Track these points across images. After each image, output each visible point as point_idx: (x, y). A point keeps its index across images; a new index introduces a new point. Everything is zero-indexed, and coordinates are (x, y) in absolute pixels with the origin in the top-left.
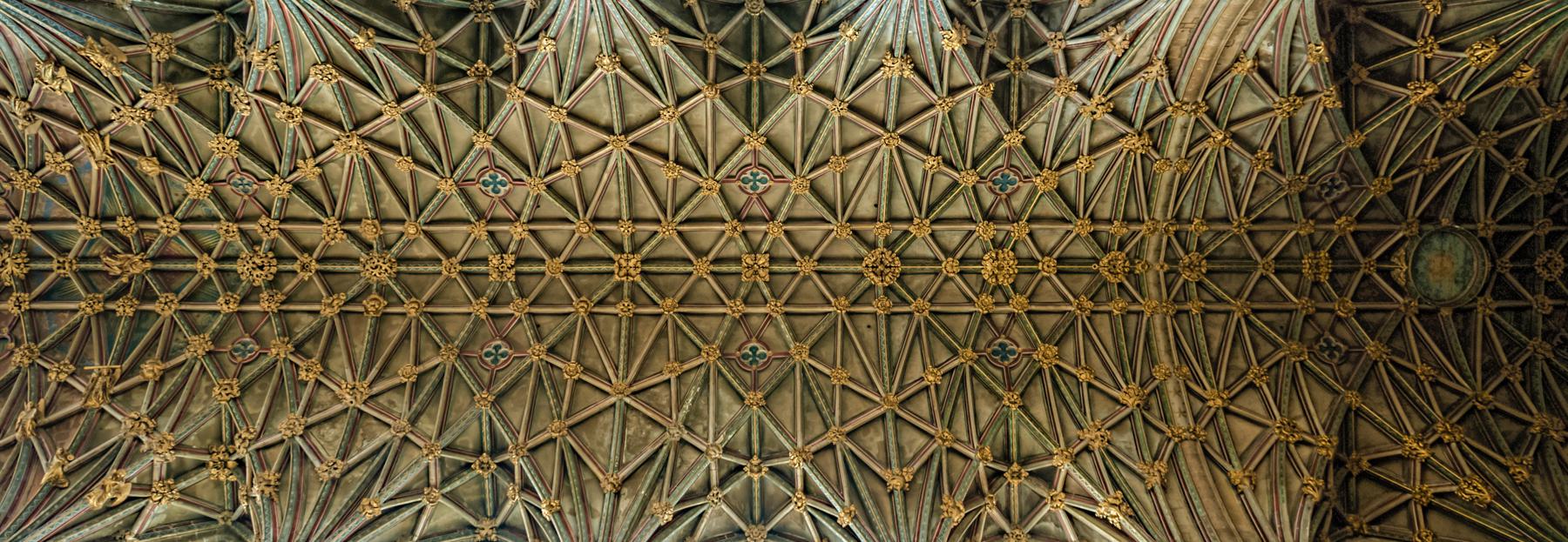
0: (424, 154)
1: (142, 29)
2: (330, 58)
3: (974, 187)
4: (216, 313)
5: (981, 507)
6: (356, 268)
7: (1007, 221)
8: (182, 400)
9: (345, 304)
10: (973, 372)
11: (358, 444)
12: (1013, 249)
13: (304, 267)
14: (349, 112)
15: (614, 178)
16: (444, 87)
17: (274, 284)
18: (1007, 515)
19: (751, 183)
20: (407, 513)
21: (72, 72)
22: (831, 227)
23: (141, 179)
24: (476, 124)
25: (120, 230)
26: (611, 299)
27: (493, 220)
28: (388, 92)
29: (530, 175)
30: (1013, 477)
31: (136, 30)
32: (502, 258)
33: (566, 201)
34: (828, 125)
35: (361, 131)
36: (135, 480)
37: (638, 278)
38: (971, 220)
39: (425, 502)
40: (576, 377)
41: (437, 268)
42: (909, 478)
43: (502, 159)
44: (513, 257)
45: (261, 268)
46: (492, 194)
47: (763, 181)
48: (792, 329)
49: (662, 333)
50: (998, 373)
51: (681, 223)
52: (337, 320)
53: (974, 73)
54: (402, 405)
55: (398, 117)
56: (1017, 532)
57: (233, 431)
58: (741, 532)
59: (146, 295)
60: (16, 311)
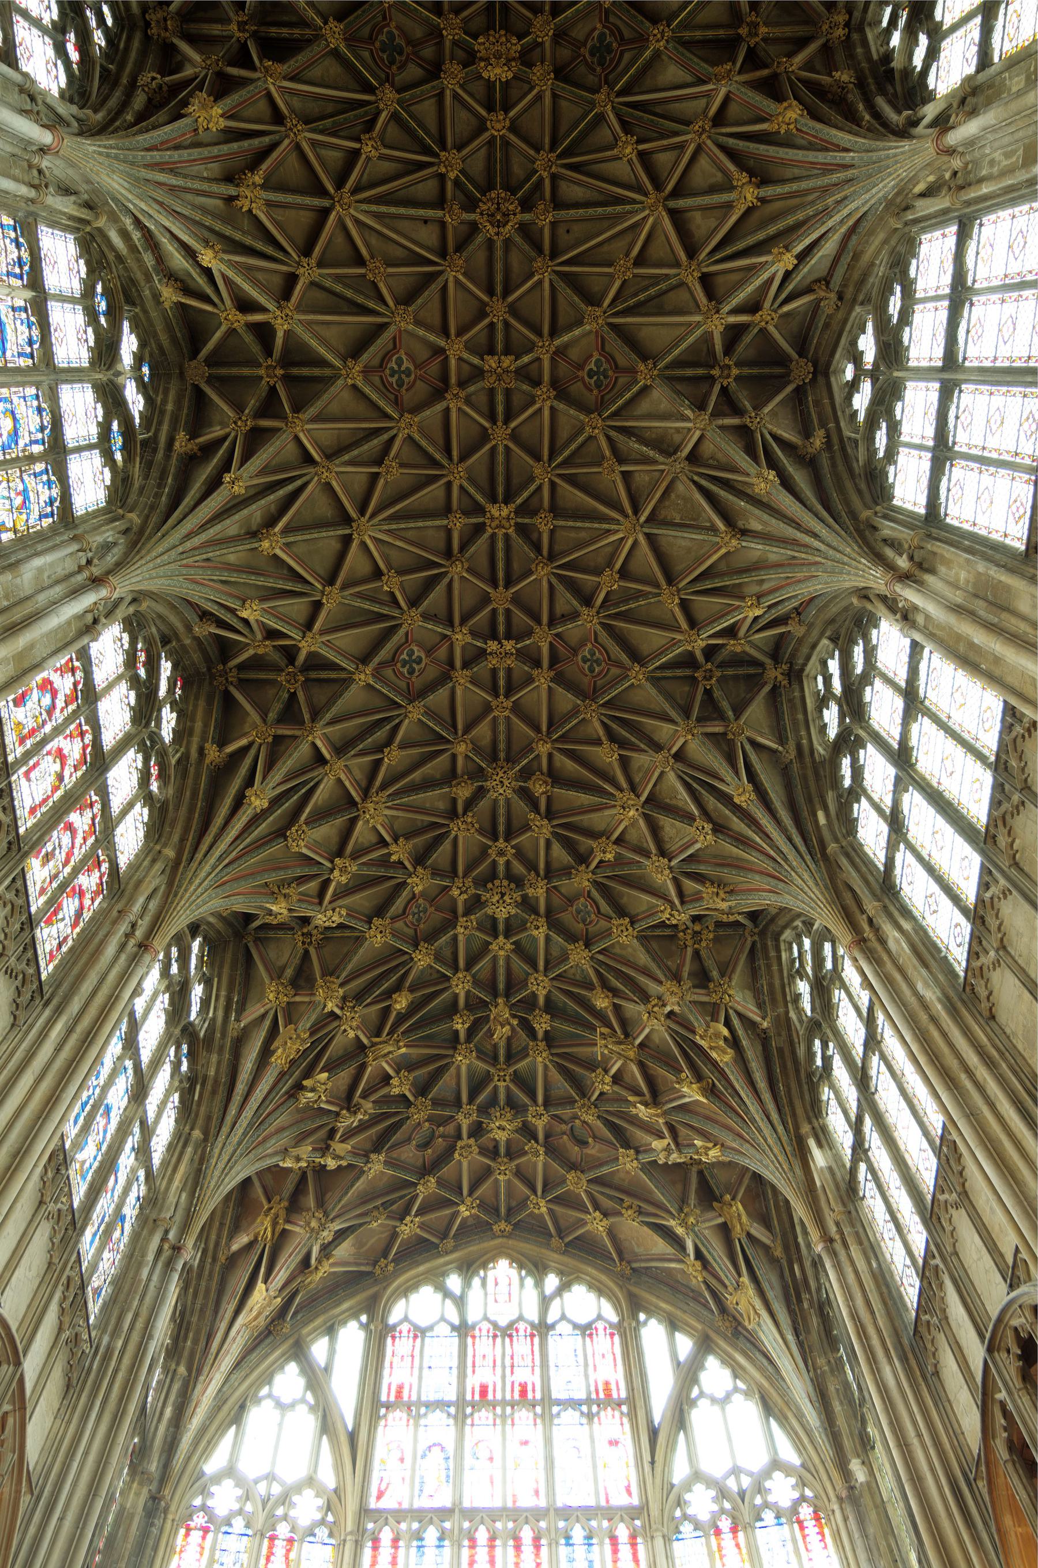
0: (381, 734)
1: (262, 1010)
2: (280, 833)
3: (399, 92)
4: (548, 938)
5: (789, 79)
7: (440, 44)
8: (632, 973)
10: (624, 92)
11: (680, 804)
12: (475, 37)
13: (501, 853)
14: (339, 812)
15: (403, 534)
16: (307, 717)
17: (518, 882)
18: (802, 43)
19: (403, 376)
20: (753, 757)
21: (308, 1074)
22: (451, 279)
23: (413, 1008)
24: (346, 682)
25: (467, 1026)
26: (535, 536)
28: (315, 773)
29: (401, 625)
30: (757, 35)
32: (491, 654)
33: (430, 584)
34: (328, 283)
35: (358, 799)
36: (708, 1019)
37: (512, 507)
38: (441, 96)
39: (742, 738)
40: (617, 576)
41: (501, 721)
42: (744, 177)
43: (384, 654)
44: (490, 643)
45: (503, 895)
46: (423, 665)
47: (400, 362)
48: (570, 328)
49: (571, 480)
50: (627, 56)
52: (555, 822)
53: (251, 88)
54: (642, 760)
55: (341, 763)
56: (825, 27)
57: (662, 925)
58: (798, 389)
59: (530, 1004)
60: (546, 1119)
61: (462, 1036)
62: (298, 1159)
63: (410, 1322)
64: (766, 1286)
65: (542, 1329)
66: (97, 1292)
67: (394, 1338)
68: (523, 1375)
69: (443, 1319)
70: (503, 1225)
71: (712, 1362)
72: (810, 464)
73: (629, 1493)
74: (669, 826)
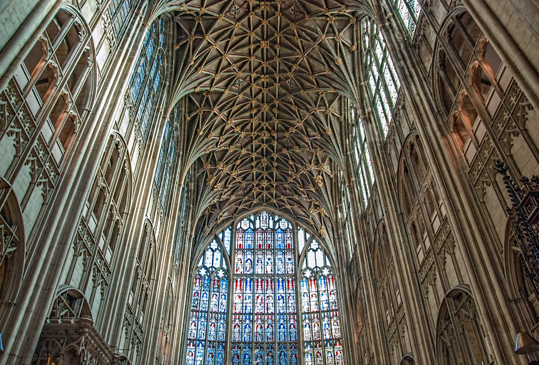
1: (203, 171)
4: (277, 145)
6: (265, 112)
9: (275, 117)
13: (265, 125)
21: (215, 185)
27: (250, 80)
31: (204, 172)
33: (244, 64)
45: (265, 134)
51: (250, 30)
52: (279, 120)
61: (254, 167)
64: (328, 227)
65: (274, 230)
68: (269, 242)
69: (250, 227)
70: (265, 204)
71: (314, 241)
72: (353, 53)
73: (292, 271)
74: (309, 129)
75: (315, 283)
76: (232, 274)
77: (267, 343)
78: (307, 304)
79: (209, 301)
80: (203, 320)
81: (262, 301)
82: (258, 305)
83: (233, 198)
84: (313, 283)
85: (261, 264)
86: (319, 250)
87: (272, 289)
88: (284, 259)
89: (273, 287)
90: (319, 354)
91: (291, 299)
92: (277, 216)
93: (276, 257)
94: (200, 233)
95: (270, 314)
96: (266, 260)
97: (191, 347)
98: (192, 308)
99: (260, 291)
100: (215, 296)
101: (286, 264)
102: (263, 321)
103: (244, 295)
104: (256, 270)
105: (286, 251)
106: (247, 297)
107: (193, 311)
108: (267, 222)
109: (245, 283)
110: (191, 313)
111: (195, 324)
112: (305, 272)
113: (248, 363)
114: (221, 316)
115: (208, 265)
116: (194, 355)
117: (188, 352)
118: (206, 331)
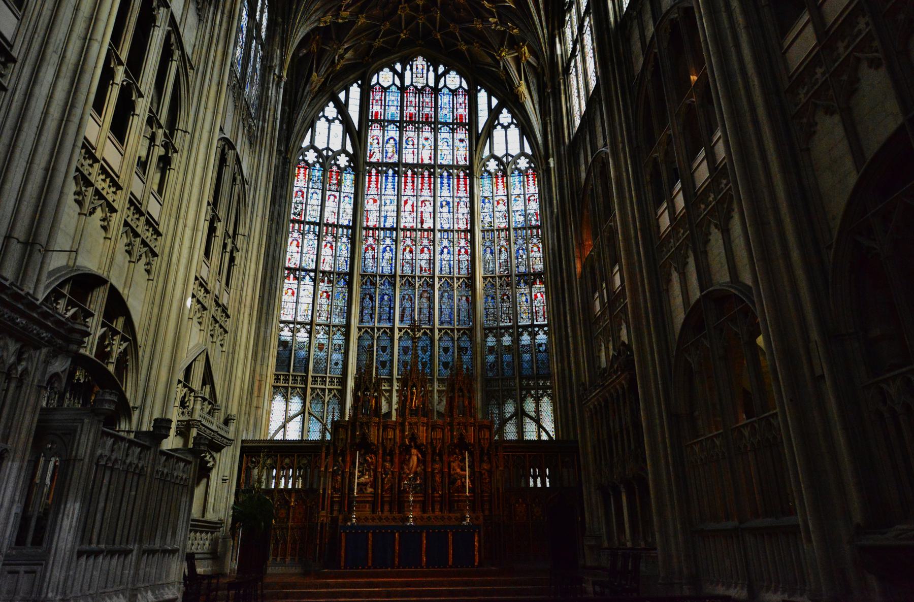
62: (325, 22)
63: (380, 85)
64: (531, 84)
65: (436, 91)
66: (253, 104)
67: (373, 92)
68: (427, 110)
69: (394, 84)
70: (420, 42)
71: (505, 111)
73: (466, 161)
75: (503, 182)
76: (361, 162)
77: (420, 278)
78: (488, 216)
79: (321, 205)
80: (311, 236)
81: (413, 209)
82: (407, 214)
83: (362, 20)
84: (500, 181)
85: (412, 147)
86: (513, 126)
87: (430, 189)
88: (451, 140)
89: (432, 185)
90: (505, 297)
91: (463, 206)
92: (441, 66)
93: (439, 136)
94: (303, 85)
95: (426, 230)
96: (422, 141)
97: (291, 281)
98: (292, 217)
99: (409, 192)
100: (332, 198)
101: (455, 148)
102: (414, 241)
103: (383, 197)
104: (404, 157)
105: (455, 127)
106: (388, 202)
107: (294, 221)
108: (425, 75)
109: (384, 178)
110: (291, 225)
111: (298, 243)
112: (488, 163)
113: (388, 309)
114: (343, 231)
115: (320, 143)
116: (295, 295)
117: (285, 289)
118: (317, 255)
